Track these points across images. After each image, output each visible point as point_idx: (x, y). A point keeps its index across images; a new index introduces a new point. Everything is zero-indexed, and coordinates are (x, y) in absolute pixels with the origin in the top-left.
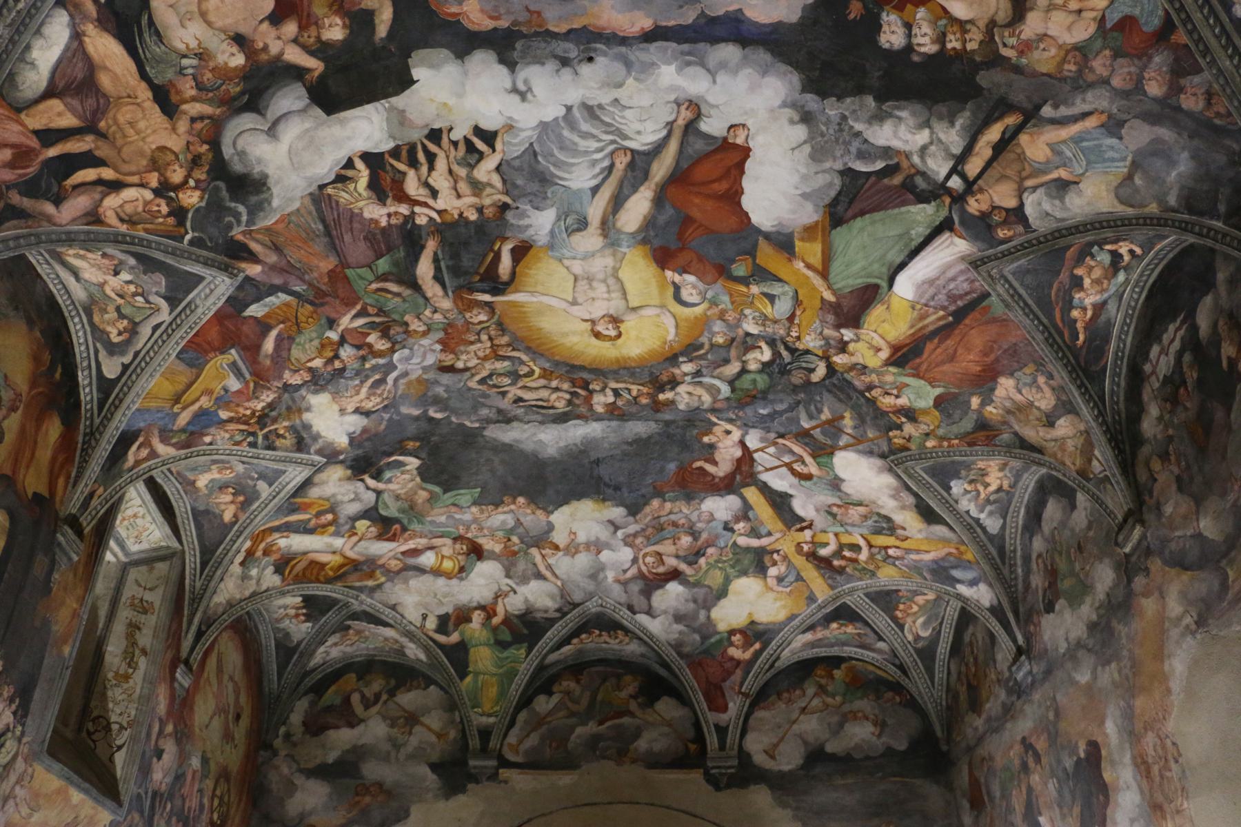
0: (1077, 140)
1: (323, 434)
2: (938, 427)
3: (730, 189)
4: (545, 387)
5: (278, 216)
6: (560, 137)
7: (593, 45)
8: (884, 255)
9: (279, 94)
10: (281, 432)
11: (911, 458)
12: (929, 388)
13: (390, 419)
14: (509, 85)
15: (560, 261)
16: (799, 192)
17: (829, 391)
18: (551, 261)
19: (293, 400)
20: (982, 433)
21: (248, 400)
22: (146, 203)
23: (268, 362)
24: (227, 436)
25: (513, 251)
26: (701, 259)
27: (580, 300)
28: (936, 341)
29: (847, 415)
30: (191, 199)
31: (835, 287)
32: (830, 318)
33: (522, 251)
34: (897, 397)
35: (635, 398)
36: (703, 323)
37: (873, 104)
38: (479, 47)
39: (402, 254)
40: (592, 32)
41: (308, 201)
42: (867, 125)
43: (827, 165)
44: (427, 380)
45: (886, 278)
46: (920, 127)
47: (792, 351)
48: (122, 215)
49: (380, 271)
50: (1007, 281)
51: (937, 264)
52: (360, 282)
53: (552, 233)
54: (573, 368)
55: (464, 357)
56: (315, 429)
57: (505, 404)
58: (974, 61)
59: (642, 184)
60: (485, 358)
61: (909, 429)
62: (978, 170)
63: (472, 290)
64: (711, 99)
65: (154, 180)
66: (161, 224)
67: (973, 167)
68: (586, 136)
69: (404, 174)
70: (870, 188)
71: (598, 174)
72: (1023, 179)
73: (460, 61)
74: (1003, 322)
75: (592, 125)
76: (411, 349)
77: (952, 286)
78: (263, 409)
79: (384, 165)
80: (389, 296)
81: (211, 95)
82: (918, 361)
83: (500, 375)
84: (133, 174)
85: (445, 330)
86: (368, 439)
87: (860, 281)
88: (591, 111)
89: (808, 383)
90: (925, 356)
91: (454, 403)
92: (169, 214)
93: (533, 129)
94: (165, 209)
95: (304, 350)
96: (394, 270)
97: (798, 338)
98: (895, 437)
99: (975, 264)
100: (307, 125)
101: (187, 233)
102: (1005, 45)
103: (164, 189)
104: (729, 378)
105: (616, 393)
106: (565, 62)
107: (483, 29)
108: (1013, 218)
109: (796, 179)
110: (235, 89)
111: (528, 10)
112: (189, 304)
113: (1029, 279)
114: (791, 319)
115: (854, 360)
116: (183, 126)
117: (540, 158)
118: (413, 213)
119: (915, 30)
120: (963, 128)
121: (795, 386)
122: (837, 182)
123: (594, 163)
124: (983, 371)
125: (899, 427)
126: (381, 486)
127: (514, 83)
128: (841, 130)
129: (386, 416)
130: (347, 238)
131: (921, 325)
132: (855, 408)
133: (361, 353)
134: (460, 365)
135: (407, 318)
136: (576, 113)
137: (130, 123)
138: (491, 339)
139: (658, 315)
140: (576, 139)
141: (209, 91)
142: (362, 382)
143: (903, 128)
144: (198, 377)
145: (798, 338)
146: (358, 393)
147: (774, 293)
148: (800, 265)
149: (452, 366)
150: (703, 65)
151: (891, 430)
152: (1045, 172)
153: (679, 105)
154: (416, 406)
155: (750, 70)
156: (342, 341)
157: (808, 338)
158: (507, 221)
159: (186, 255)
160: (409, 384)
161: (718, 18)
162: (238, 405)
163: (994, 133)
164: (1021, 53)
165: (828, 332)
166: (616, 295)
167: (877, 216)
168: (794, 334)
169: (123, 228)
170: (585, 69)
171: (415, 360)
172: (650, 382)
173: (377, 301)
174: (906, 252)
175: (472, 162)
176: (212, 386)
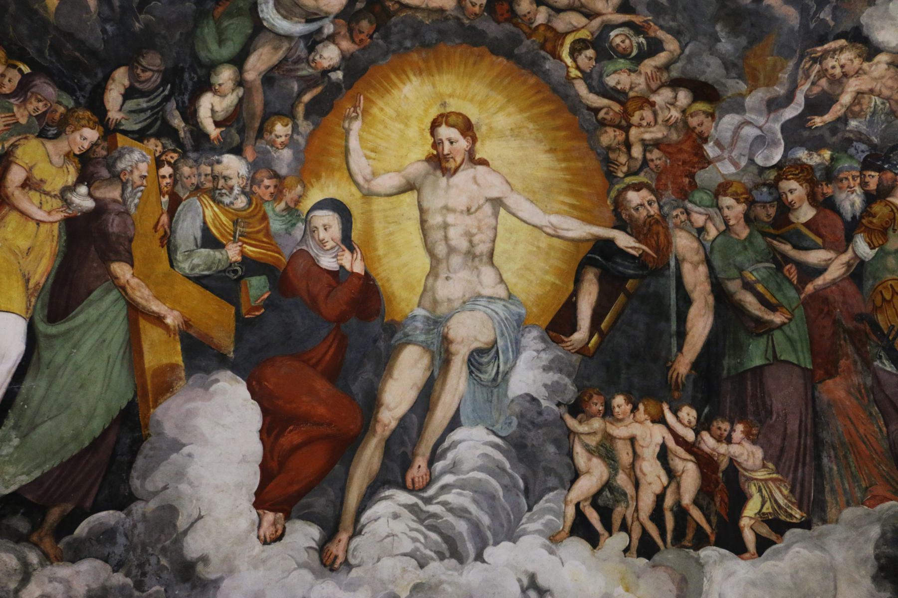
3: (277, 437)
5: (878, 508)
6: (494, 516)
8: (50, 385)
15: (510, 296)
16: (185, 450)
17: (93, 53)
18: (522, 297)
25: (573, 327)
27: (488, 209)
31: (114, 294)
32: (114, 225)
39: (727, 362)
41: (831, 512)
42: (108, 584)
43: (153, 504)
44: (740, 77)
45: (42, 341)
47: (167, 132)
49: (762, 341)
52: (795, 336)
53: (517, 352)
55: (675, 114)
59: (394, 432)
60: (644, 101)
63: (640, 261)
64: (308, 576)
68: (461, 512)
69: (696, 502)
75: (453, 528)
76: (751, 161)
80: (760, 288)
83: (625, 55)
85: (694, 186)
87: (80, 319)
89: (131, 62)
93: (525, 533)
97: (159, 163)
104: (262, 38)
109: (192, 471)
114: (175, 202)
115: (62, 145)
117: (521, 483)
118: (697, 432)
121: (152, 47)
122: (136, 483)
123: (453, 468)
128: (141, 566)
129: (826, 15)
130: (793, 425)
133: (828, 190)
134: (684, 97)
135: (744, 232)
138: (628, 145)
139: (375, 174)
140: (473, 508)
142: (843, 120)
145: (159, 163)
146: (859, 94)
147: (204, 251)
149: (695, 99)
153: (346, 563)
156: (852, 227)
157: (143, 168)
158: (575, 382)
160: (771, 81)
165: (112, 193)
166: (435, 220)
167: (73, 449)
168: (166, 170)
171: (750, 132)
172: (389, 14)
173: (780, 288)
174: (19, 400)
175: (607, 493)
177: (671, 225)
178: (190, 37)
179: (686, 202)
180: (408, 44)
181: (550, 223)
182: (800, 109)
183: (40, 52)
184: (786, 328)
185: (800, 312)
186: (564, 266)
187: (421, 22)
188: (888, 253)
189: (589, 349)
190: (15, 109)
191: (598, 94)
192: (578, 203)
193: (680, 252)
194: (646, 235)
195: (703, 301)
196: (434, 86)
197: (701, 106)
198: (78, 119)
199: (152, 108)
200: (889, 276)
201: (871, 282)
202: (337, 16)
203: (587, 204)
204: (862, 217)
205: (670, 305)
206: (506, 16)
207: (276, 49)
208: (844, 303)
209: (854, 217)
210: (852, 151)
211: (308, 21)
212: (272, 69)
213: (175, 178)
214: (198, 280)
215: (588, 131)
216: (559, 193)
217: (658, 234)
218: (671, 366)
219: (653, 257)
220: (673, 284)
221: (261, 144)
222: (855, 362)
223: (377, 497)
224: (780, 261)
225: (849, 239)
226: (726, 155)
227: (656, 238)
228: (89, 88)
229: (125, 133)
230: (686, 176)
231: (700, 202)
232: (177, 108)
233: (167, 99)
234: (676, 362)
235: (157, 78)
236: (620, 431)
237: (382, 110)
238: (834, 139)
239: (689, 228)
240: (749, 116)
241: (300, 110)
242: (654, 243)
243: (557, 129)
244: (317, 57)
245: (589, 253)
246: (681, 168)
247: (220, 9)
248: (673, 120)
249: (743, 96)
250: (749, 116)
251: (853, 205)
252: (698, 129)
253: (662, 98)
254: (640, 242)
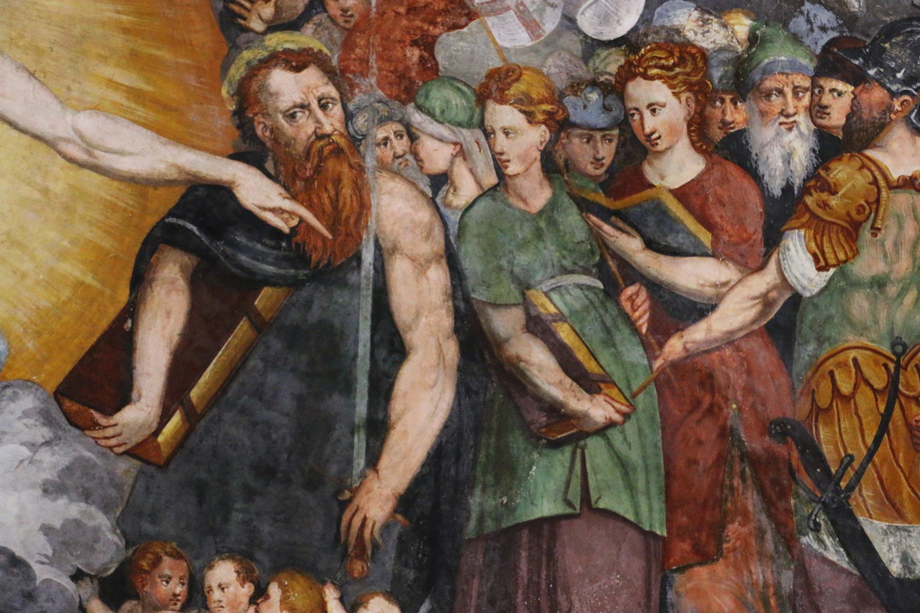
39: (476, 501)
49: (562, 458)
52: (634, 456)
76: (569, 22)
80: (564, 333)
158: (119, 523)
173: (609, 341)
177: (370, 162)
179: (410, 108)
181: (76, 131)
184: (615, 435)
185: (647, 402)
186: (107, 243)
188: (856, 284)
189: (158, 446)
192: (149, 88)
193: (388, 229)
194: (308, 181)
195: (434, 351)
200: (852, 339)
201: (811, 347)
203: (171, 93)
204: (805, 190)
205: (356, 355)
208: (749, 390)
209: (788, 189)
210: (799, 24)
216: (104, 59)
217: (338, 181)
218: (350, 500)
219: (324, 238)
222: (760, 534)
227: (332, 193)
230: (414, 43)
231: (443, 112)
234: (363, 492)
239: (412, 173)
242: (327, 201)
245: (171, 214)
246: (405, 22)
251: (788, 159)
254: (294, 197)
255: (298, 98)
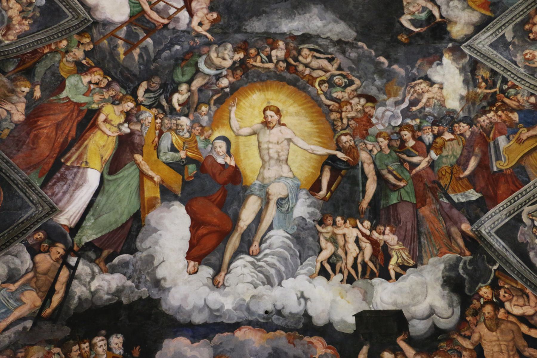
0: (8, 312)
1: (457, 71)
2: (60, 61)
3: (197, 230)
4: (314, 69)
5: (443, 257)
6: (286, 267)
7: (264, 321)
8: (107, 199)
9: (422, 333)
10: (483, 84)
11: (75, 27)
12: (70, 96)
13: (413, 67)
14: (309, 303)
15: (294, 177)
16: (159, 232)
17: (135, 75)
18: (299, 177)
19: (469, 112)
20: (28, 65)
21: (497, 123)
22: (510, 301)
23: (477, 150)
24: (519, 96)
25: (320, 190)
26: (214, 176)
27: (286, 142)
28: (70, 139)
29: (122, 57)
30: (485, 291)
31: (135, 167)
32: (137, 140)
33: (315, 188)
34: (90, 83)
35: (258, 54)
36: (214, 123)
37: (123, 299)
38: (320, 327)
39: (382, 202)
40: (265, 329)
41: (425, 260)
42: (125, 285)
43: (145, 254)
44: (384, 93)
45: (105, 182)
46: (96, 291)
47: (160, 106)
48: (526, 300)
49: (396, 194)
50: (32, 202)
51: (75, 202)
52: (409, 191)
53: (297, 199)
54: (293, 83)
55: (360, 107)
56: (462, 78)
57: (340, 59)
58: (73, 340)
59: (245, 231)
60: (348, 103)
61: (79, 53)
62: (61, 273)
63: (347, 163)
64: (207, 289)
65: (501, 314)
66: (508, 284)
67: (64, 274)
68: (272, 266)
69: (371, 260)
70: (121, 242)
71: (268, 239)
72: (35, 276)
73: (331, 321)
74: (30, 167)
75: (269, 272)
76: (390, 124)
77: (65, 187)
78: (489, 112)
79: (379, 269)
80: (395, 172)
81: (456, 348)
82: (79, 118)
83: (340, 86)
84: (511, 322)
85: (367, 134)
86: (430, 54)
87: (121, 175)
88: (269, 281)
89: (148, 79)
90: (75, 124)
91: (371, 67)
92: (501, 288)
93: (299, 274)
94: (502, 292)
95: (453, 150)
96: (388, 191)
98: (88, 44)
99: (54, 210)
100: (413, 309)
101: (495, 270)
102: (59, 354)
103: (498, 305)
104: (199, 75)
105: (269, 57)
106: (279, 313)
107: (317, 337)
108: (36, 247)
109: (161, 242)
110: (443, 344)
111: (294, 345)
112: (509, 216)
113: (19, 203)
114: (161, 133)
116: (475, 337)
117: (298, 254)
118: (371, 231)
119: (105, 348)
120: (73, 298)
121: (157, 75)
122: (138, 244)
123: (270, 247)
124: (36, 122)
125: (87, 54)
126: (430, 6)
127: (306, 304)
128: (138, 279)
129: (415, 71)
130: (409, 226)
131: (81, 150)
132: (117, 64)
133: (419, 134)
134: (363, 101)
135: (387, 151)
136: (276, 281)
137: (502, 352)
138: (341, 119)
139: (240, 128)
140: (278, 264)
141: (456, 350)
142: (424, 108)
143: (106, 288)
144: (522, 157)
145: (156, 118)
146: (429, 99)
147: (171, 153)
148: (157, 179)
149: (367, 101)
150: (211, 310)
151: (93, 50)
152: (24, 285)
153: (223, 284)
154: (395, 73)
155: (187, 309)
156: (429, 147)
157: (150, 119)
158: (320, 211)
159: (500, 257)
160: (396, 95)
161: (203, 339)
162: (505, 122)
163: (56, 299)
164: (49, 352)
165: (137, 127)
166: (264, 146)
167: (114, 227)
168: (159, 121)
169: (528, 291)
170: (270, 308)
171: (389, 114)
172: (248, 69)
173: (402, 172)
174: (95, 204)
175: (334, 257)
176: (516, 145)
177: (359, 149)
178: (172, 72)
180: (255, 80)
182: (407, 105)
183: (116, 74)
184: (405, 188)
185: (410, 181)
186: (316, 165)
187: (261, 72)
188: (443, 157)
190: (104, 93)
191: (329, 100)
194: (349, 153)
196: (265, 95)
197: (370, 104)
198: (127, 99)
199: (155, 97)
200: (444, 166)
201: (437, 168)
202: (228, 69)
203: (326, 141)
204: (432, 144)
206: (294, 71)
207: (204, 79)
208: (428, 177)
209: (430, 144)
210: (427, 119)
211: (217, 70)
212: (202, 86)
213: (162, 124)
214: (168, 164)
215: (326, 113)
217: (354, 152)
220: (360, 172)
221: (196, 114)
222: (433, 200)
223: (237, 258)
224: (402, 162)
225: (428, 152)
226: (380, 122)
228: (132, 88)
229: (144, 105)
232: (165, 98)
233: (161, 94)
235: (158, 87)
236: (339, 231)
237: (244, 103)
238: (421, 115)
239: (366, 150)
240: (388, 108)
241: (212, 102)
243: (313, 113)
244: (220, 83)
247: (184, 64)
248: (359, 109)
249: (385, 100)
250: (388, 108)
251: (429, 139)
252: (369, 113)
253: (355, 101)
254: (347, 155)
255: (346, 140)
